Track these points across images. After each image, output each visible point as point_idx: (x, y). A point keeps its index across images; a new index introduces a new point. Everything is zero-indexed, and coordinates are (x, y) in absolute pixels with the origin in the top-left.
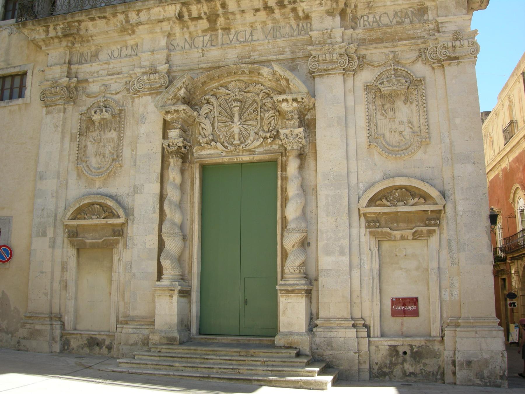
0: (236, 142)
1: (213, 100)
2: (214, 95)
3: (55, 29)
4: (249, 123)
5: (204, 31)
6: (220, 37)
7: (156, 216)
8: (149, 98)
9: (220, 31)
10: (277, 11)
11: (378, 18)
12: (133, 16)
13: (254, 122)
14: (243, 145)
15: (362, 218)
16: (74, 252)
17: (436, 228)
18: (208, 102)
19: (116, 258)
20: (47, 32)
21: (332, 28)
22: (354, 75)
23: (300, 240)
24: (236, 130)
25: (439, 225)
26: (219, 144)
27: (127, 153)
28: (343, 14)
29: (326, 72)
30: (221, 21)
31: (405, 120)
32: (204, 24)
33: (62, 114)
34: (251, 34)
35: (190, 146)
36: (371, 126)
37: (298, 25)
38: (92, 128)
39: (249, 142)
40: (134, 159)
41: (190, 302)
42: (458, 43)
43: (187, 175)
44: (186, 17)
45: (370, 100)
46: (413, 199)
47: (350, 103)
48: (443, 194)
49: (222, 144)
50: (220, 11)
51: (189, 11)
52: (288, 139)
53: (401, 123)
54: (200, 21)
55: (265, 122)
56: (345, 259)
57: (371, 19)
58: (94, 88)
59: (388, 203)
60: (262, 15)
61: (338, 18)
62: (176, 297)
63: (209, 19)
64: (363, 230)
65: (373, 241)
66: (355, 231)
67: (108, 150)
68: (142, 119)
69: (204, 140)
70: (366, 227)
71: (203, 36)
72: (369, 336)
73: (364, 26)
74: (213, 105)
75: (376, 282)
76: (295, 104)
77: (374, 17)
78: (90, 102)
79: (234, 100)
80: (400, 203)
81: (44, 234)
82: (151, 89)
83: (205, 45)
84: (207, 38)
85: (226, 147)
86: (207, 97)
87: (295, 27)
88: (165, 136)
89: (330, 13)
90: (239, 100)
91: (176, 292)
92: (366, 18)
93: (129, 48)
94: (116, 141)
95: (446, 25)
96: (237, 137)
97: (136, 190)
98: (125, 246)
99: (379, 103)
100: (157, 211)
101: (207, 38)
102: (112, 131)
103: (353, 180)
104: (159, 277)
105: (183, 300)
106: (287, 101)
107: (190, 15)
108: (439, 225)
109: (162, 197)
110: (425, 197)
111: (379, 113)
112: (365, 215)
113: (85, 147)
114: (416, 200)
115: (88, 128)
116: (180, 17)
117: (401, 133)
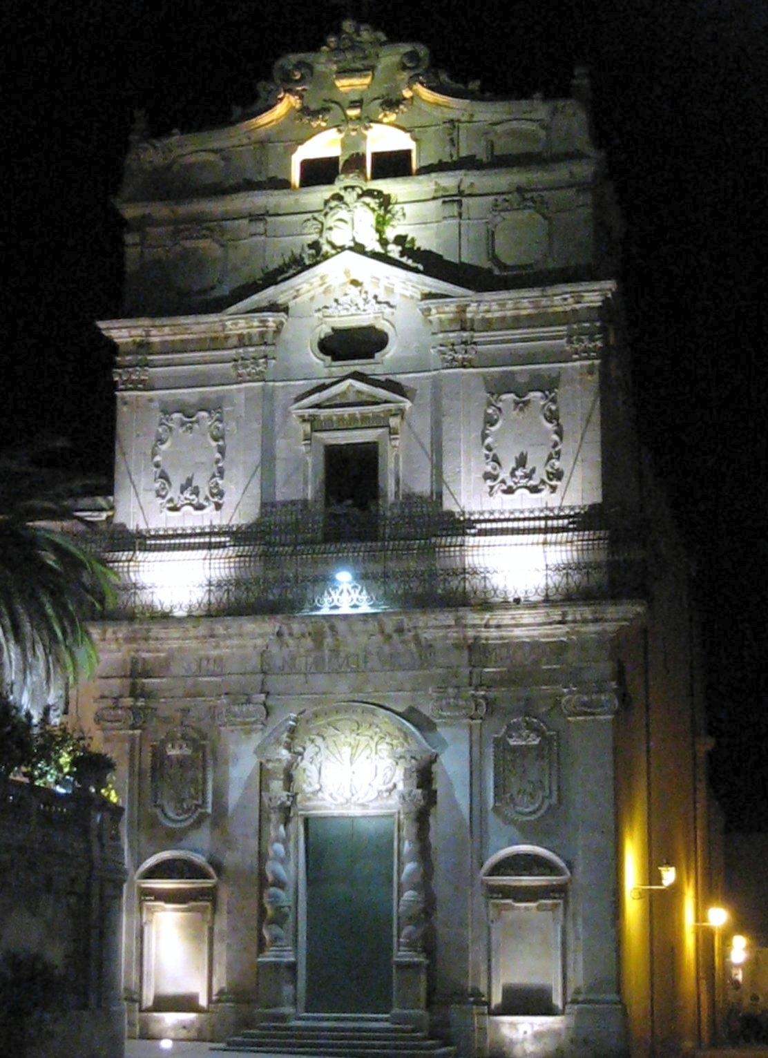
3: (114, 633)
10: (395, 636)
12: (220, 629)
21: (458, 667)
30: (329, 640)
32: (308, 642)
34: (365, 662)
50: (328, 632)
51: (290, 629)
54: (303, 640)
60: (378, 638)
61: (466, 653)
71: (306, 657)
83: (309, 667)
84: (310, 660)
87: (416, 656)
92: (498, 651)
93: (212, 662)
107: (291, 635)
116: (279, 634)
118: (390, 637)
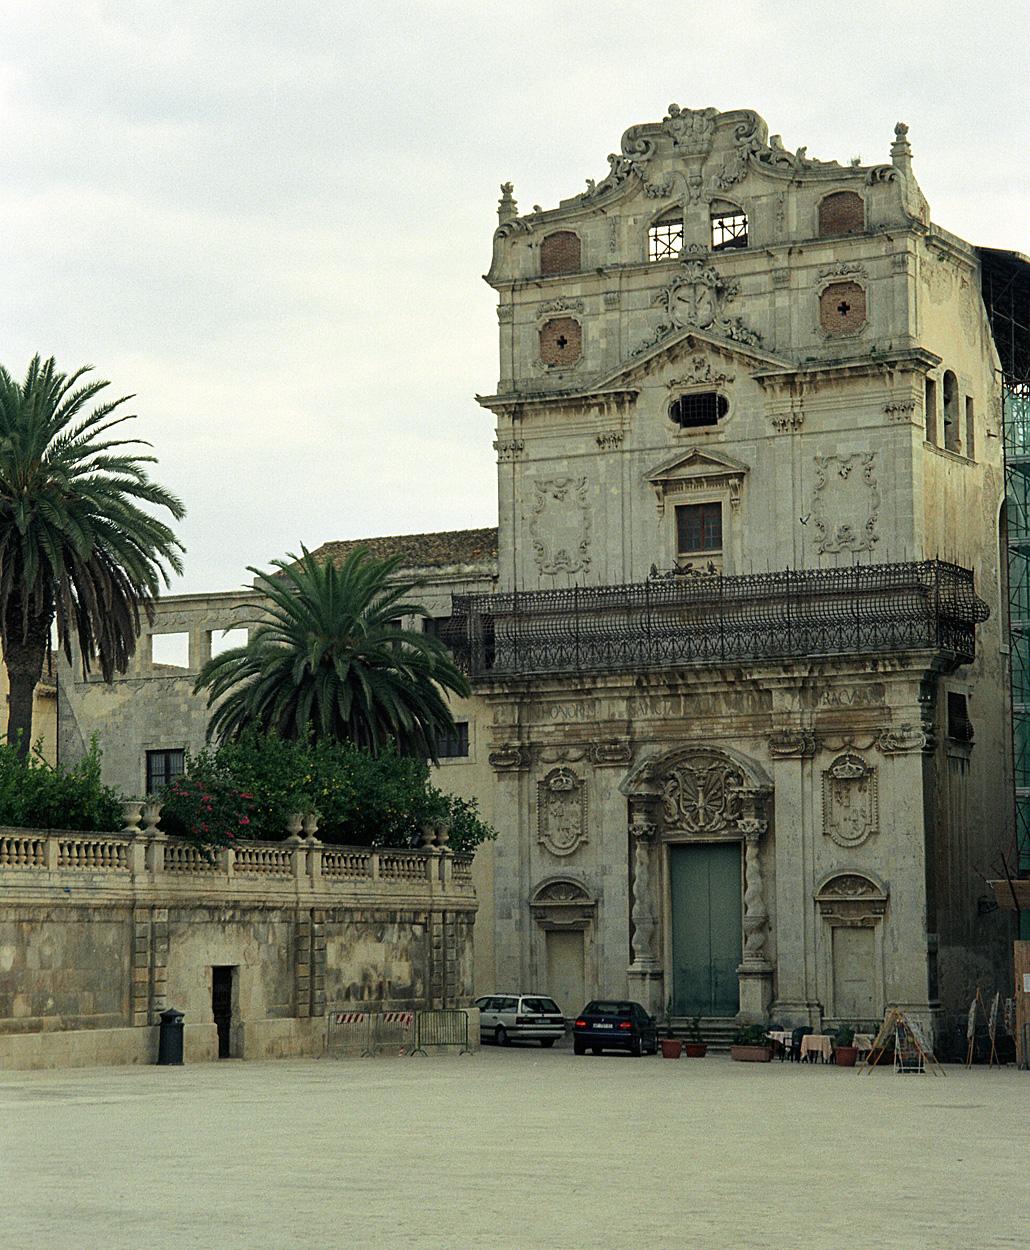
0: (702, 824)
1: (678, 775)
2: (679, 769)
4: (715, 803)
5: (664, 696)
6: (683, 703)
7: (626, 898)
8: (611, 771)
9: (682, 698)
10: (737, 683)
11: (837, 695)
13: (718, 803)
14: (708, 827)
15: (818, 904)
16: (543, 934)
17: (882, 916)
18: (673, 777)
19: (587, 940)
20: (493, 688)
22: (812, 759)
23: (764, 925)
24: (701, 811)
25: (884, 913)
26: (684, 825)
27: (592, 829)
28: (803, 690)
29: (786, 757)
31: (858, 809)
33: (517, 782)
35: (656, 827)
36: (826, 813)
37: (760, 698)
38: (552, 799)
39: (714, 823)
40: (600, 836)
41: (663, 984)
42: (905, 734)
43: (655, 856)
44: (645, 684)
45: (828, 788)
46: (862, 886)
47: (808, 788)
48: (887, 886)
49: (688, 824)
52: (745, 828)
53: (854, 811)
55: (729, 805)
56: (800, 944)
57: (831, 697)
58: (548, 754)
59: (840, 892)
62: (647, 981)
63: (669, 687)
64: (819, 916)
65: (827, 925)
66: (810, 917)
67: (573, 820)
68: (604, 794)
69: (670, 820)
70: (822, 913)
72: (822, 1015)
73: (825, 703)
74: (677, 781)
75: (830, 966)
76: (751, 796)
77: (834, 694)
78: (548, 769)
79: (699, 778)
80: (849, 892)
81: (509, 916)
82: (612, 761)
84: (669, 704)
85: (692, 828)
86: (672, 772)
87: (757, 698)
88: (630, 820)
89: (788, 689)
90: (704, 779)
91: (648, 976)
94: (580, 814)
95: (898, 712)
96: (701, 818)
97: (604, 871)
98: (596, 928)
99: (835, 790)
100: (627, 893)
101: (669, 704)
102: (575, 803)
103: (809, 868)
104: (632, 963)
105: (655, 982)
106: (742, 791)
108: (884, 913)
109: (631, 879)
110: (873, 887)
111: (834, 800)
112: (820, 902)
113: (546, 819)
114: (864, 889)
115: (547, 798)
117: (854, 821)
118: (733, 683)
